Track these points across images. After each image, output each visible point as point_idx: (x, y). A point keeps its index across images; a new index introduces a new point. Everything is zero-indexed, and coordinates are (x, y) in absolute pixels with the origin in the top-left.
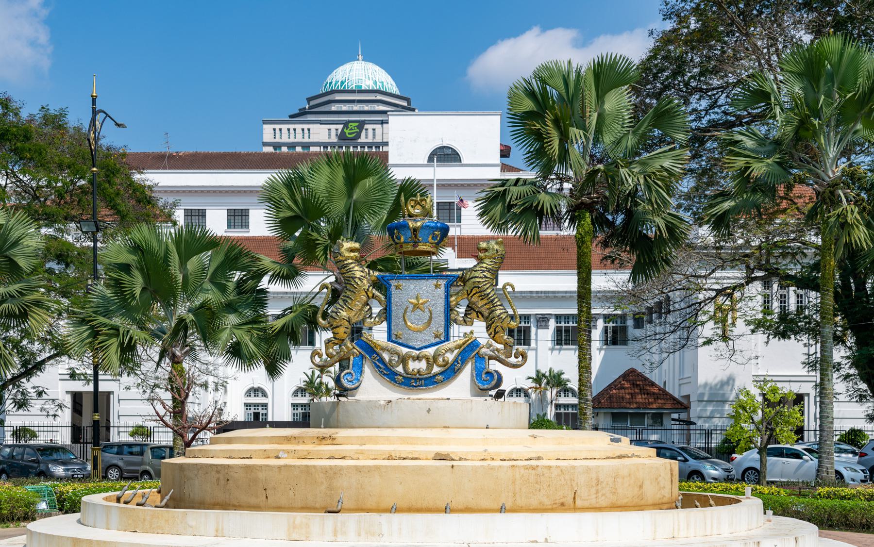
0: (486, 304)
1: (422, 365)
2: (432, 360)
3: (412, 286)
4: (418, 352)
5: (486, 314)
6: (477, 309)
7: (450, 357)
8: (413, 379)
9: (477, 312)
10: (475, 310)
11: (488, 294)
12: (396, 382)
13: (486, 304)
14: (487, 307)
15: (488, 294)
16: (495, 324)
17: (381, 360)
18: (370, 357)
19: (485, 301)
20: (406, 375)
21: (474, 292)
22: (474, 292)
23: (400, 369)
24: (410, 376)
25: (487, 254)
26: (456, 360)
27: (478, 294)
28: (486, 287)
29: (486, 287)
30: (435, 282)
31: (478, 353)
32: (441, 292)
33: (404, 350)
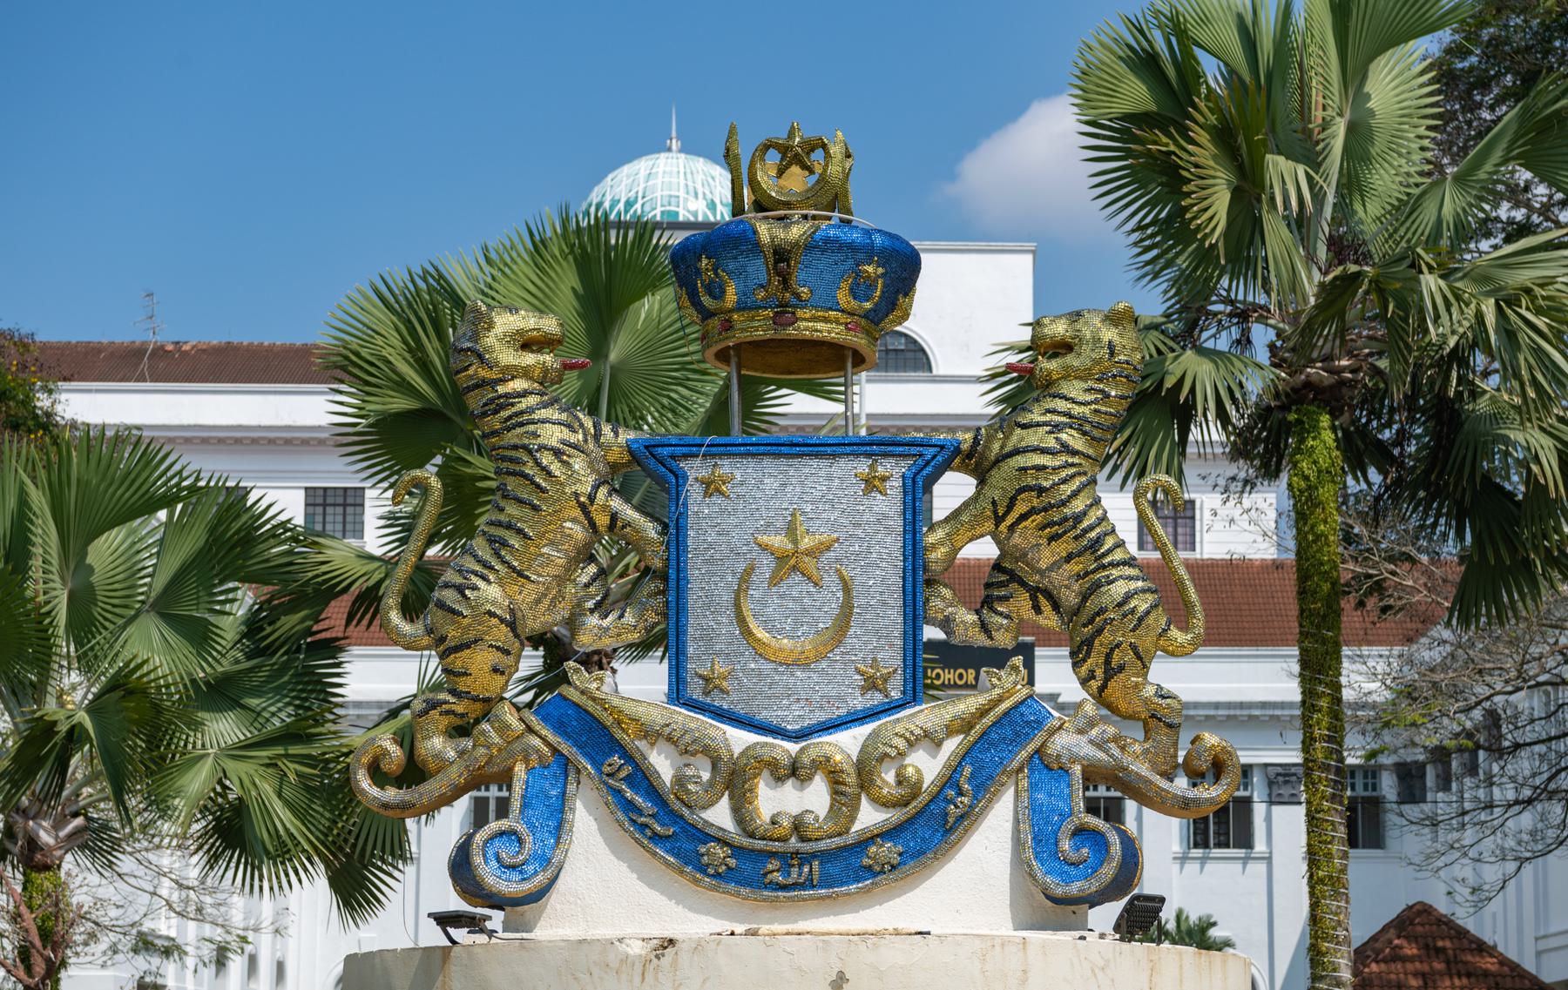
0: (1069, 558)
1: (815, 799)
2: (851, 779)
3: (771, 484)
4: (793, 748)
5: (1070, 598)
6: (1034, 580)
7: (928, 766)
8: (773, 854)
9: (1034, 592)
10: (1023, 584)
11: (1078, 518)
12: (702, 869)
13: (1069, 558)
14: (1074, 567)
15: (1078, 518)
16: (1107, 637)
17: (642, 778)
18: (597, 765)
19: (1062, 548)
20: (746, 842)
21: (1020, 508)
22: (1020, 508)
23: (720, 815)
24: (760, 844)
25: (1071, 360)
26: (950, 779)
27: (1039, 518)
28: (1067, 489)
29: (1067, 489)
30: (863, 466)
31: (1038, 752)
32: (888, 504)
33: (739, 739)
